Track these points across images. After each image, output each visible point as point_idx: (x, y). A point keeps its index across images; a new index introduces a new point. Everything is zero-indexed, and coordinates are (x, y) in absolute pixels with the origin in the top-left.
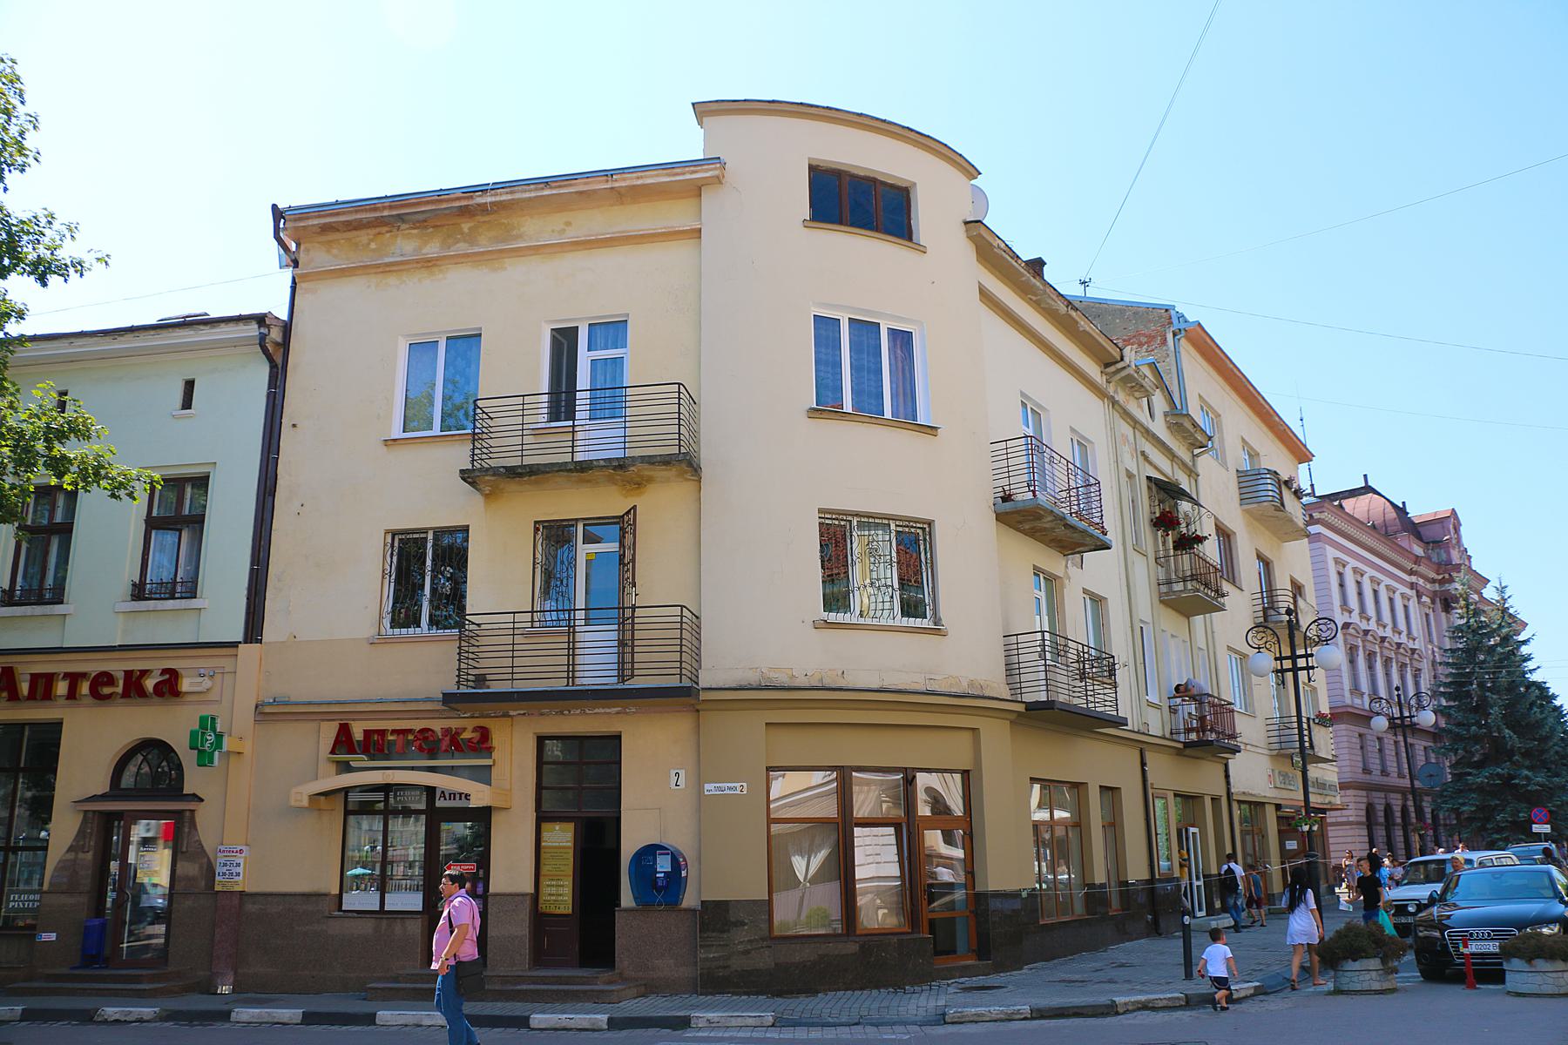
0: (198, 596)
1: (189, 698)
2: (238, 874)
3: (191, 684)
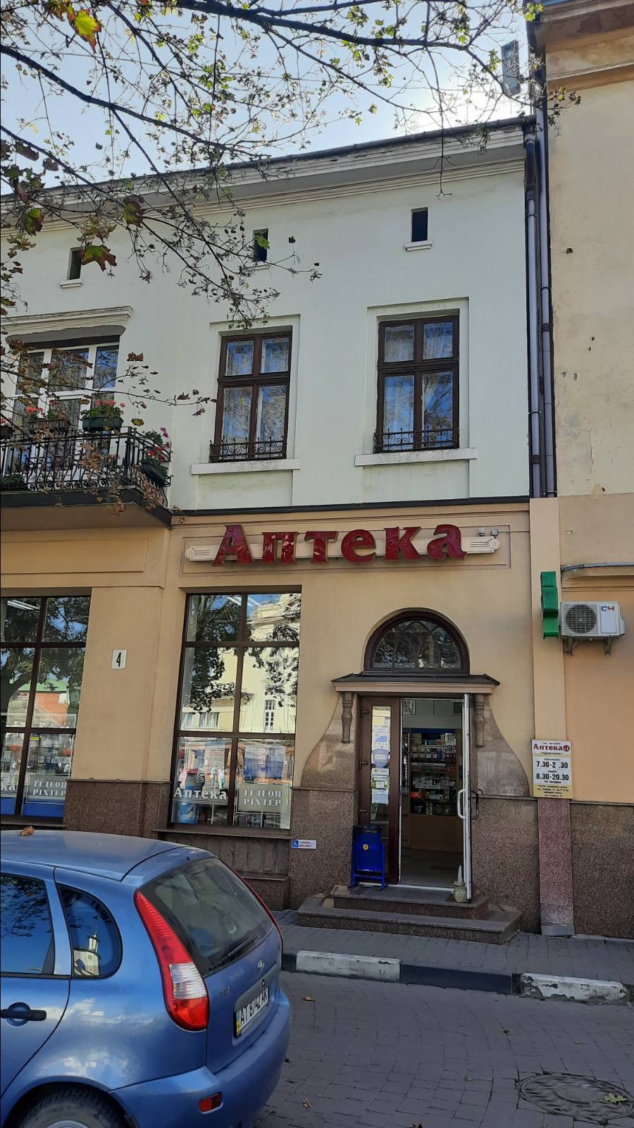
0: (460, 446)
1: (468, 562)
2: (566, 777)
3: (474, 545)
